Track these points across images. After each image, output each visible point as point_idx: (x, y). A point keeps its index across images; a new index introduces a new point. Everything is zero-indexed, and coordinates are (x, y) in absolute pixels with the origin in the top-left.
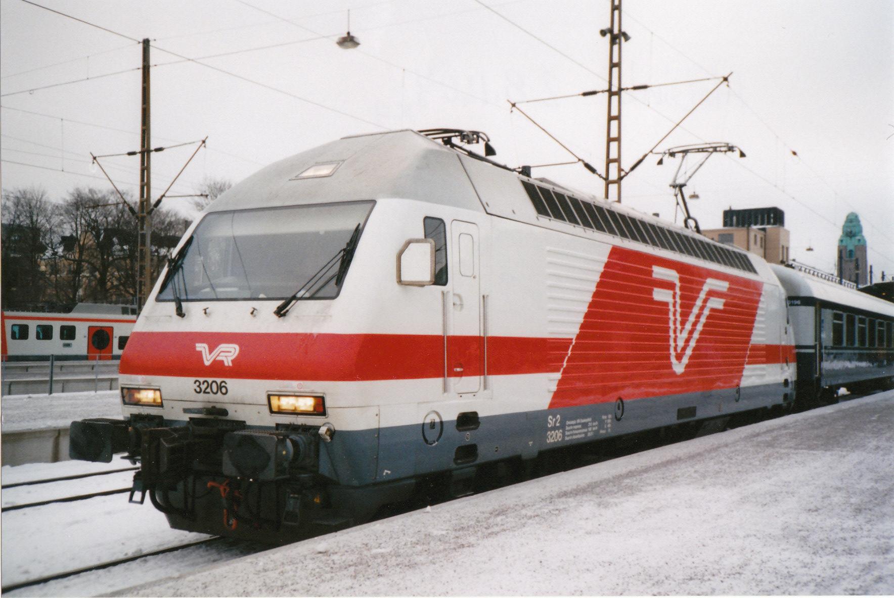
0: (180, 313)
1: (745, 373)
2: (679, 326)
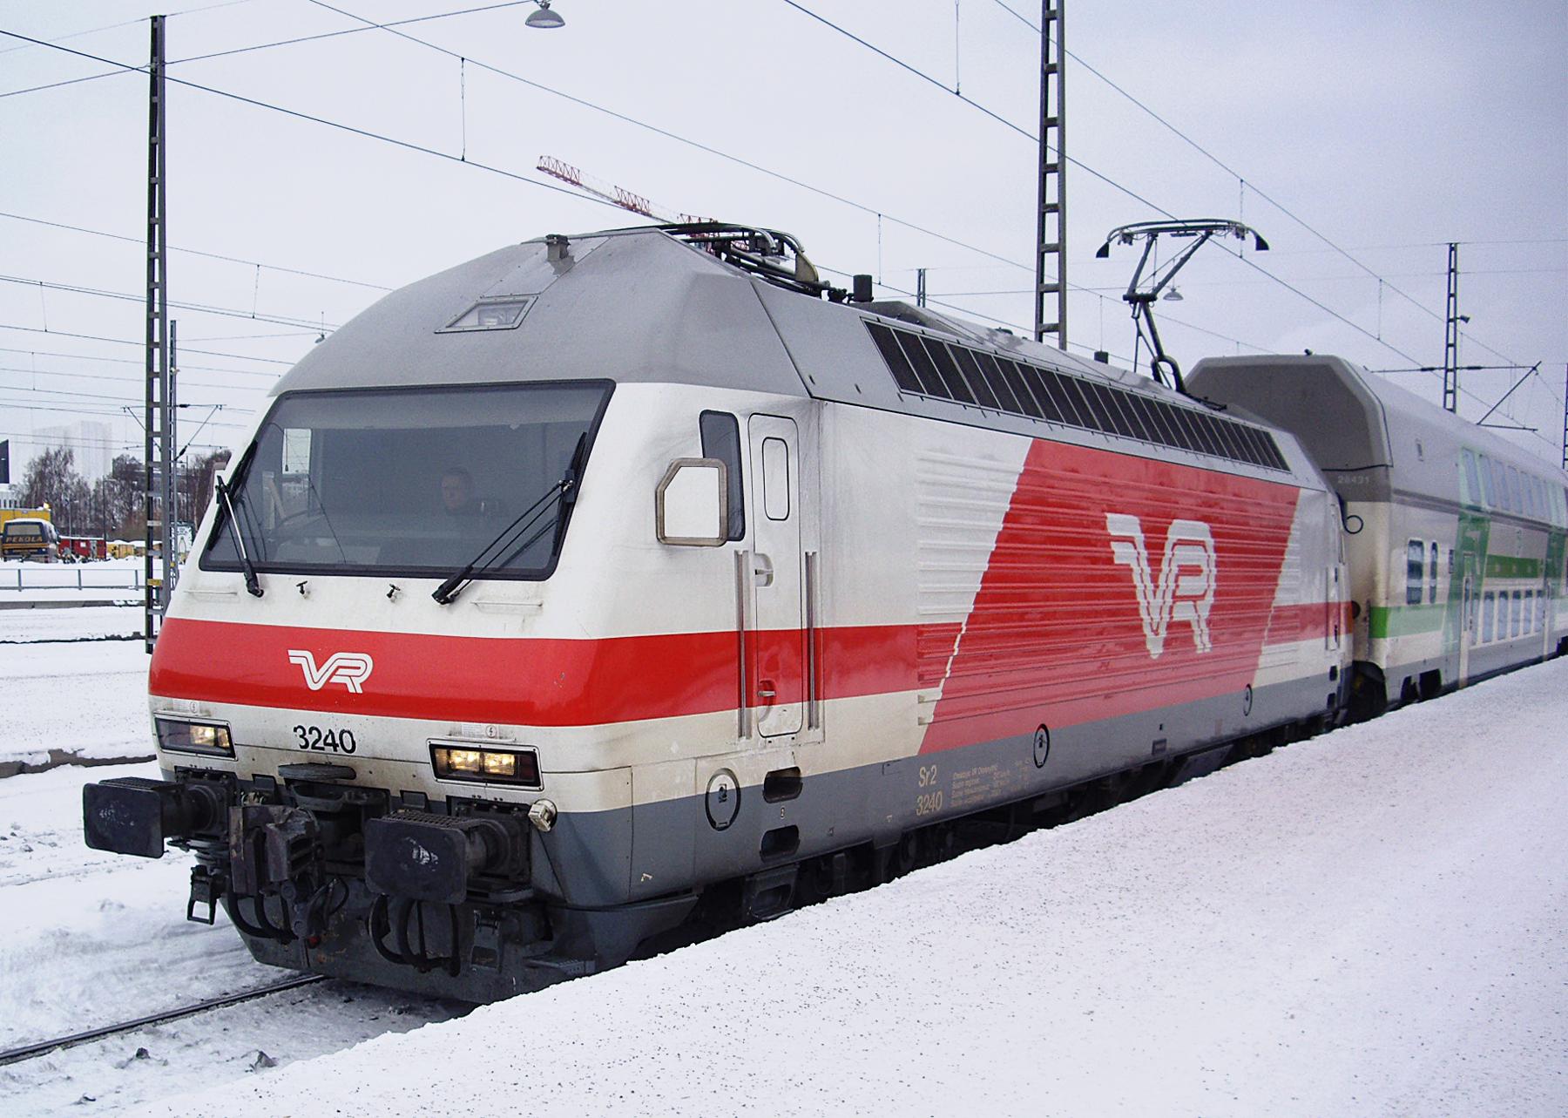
0: (255, 590)
1: (1262, 660)
2: (1150, 586)
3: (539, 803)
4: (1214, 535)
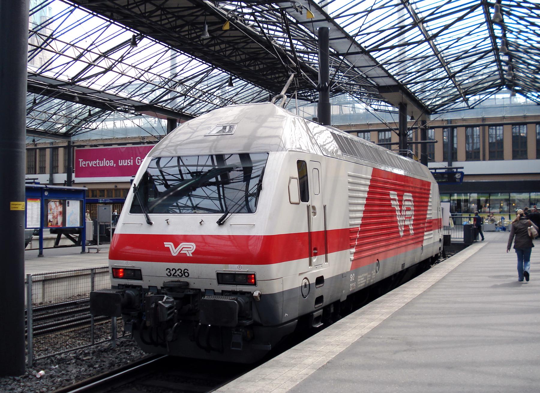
4: (413, 197)
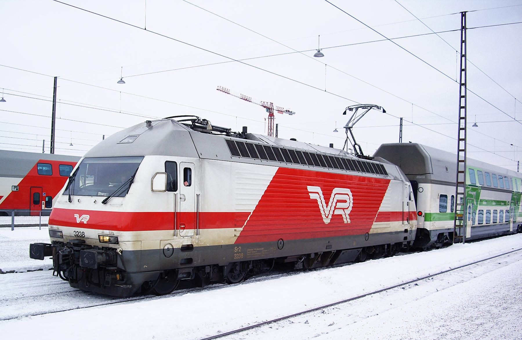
0: (70, 200)
1: (373, 227)
2: (325, 205)
3: (120, 248)
